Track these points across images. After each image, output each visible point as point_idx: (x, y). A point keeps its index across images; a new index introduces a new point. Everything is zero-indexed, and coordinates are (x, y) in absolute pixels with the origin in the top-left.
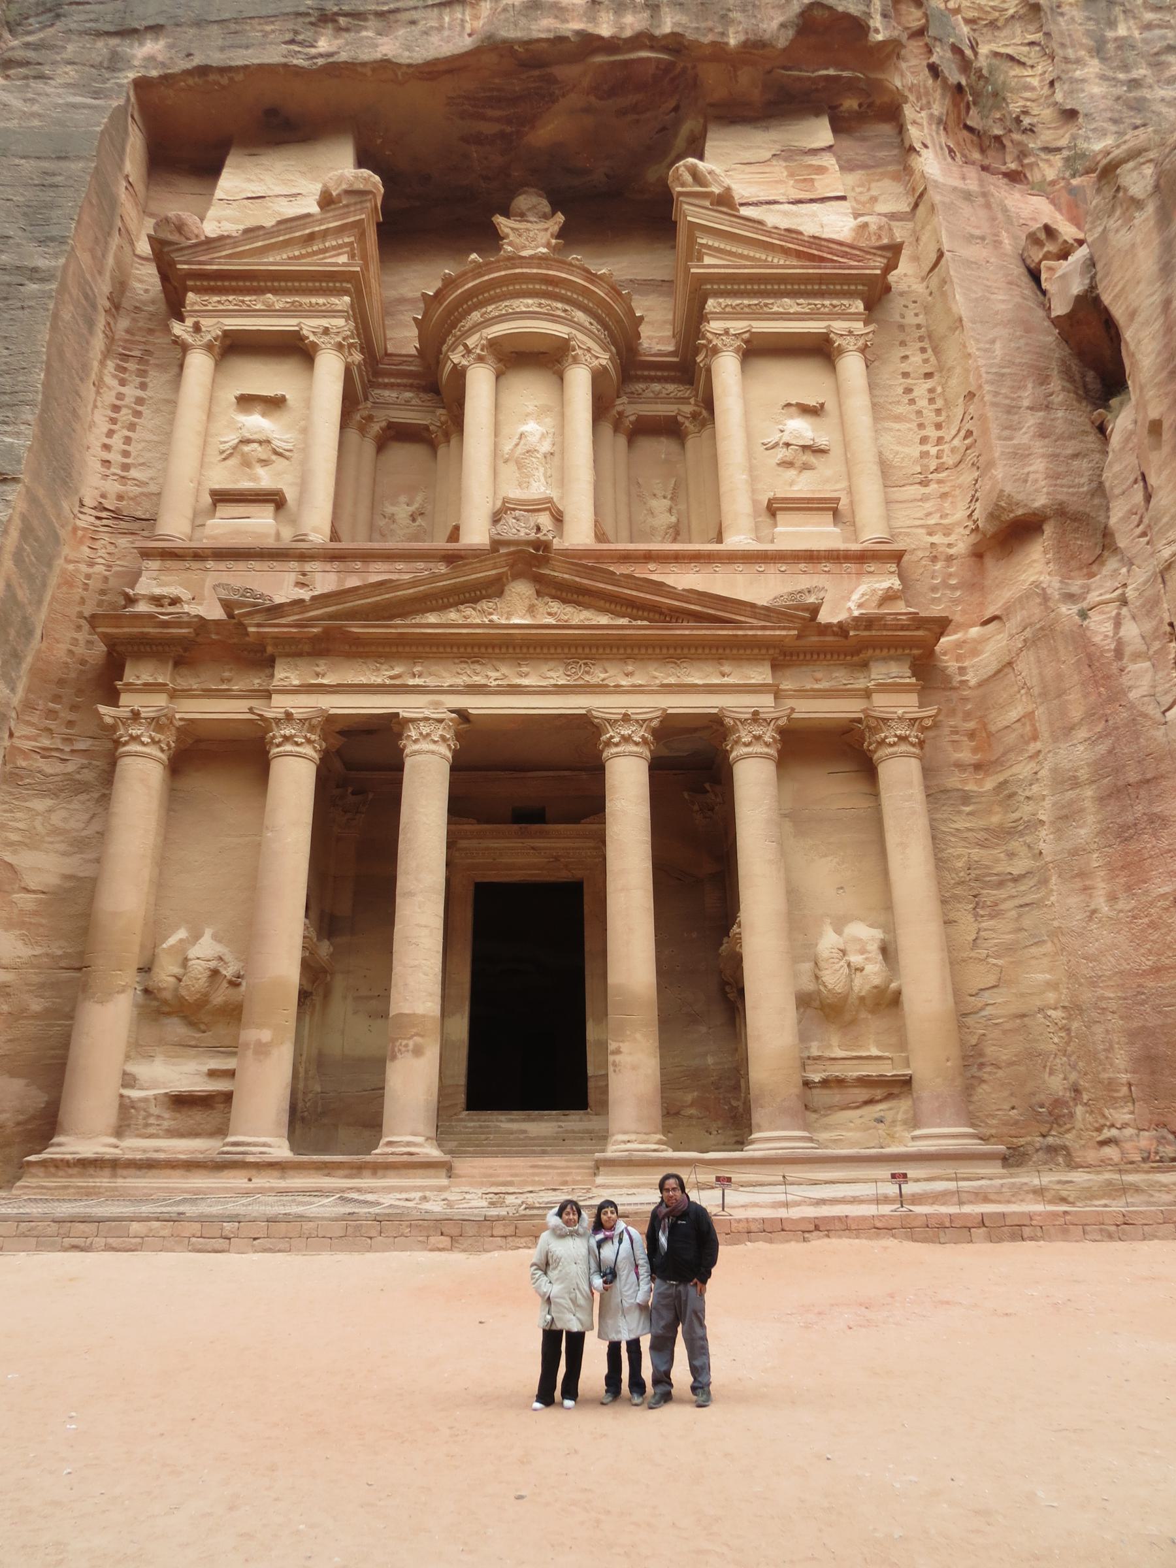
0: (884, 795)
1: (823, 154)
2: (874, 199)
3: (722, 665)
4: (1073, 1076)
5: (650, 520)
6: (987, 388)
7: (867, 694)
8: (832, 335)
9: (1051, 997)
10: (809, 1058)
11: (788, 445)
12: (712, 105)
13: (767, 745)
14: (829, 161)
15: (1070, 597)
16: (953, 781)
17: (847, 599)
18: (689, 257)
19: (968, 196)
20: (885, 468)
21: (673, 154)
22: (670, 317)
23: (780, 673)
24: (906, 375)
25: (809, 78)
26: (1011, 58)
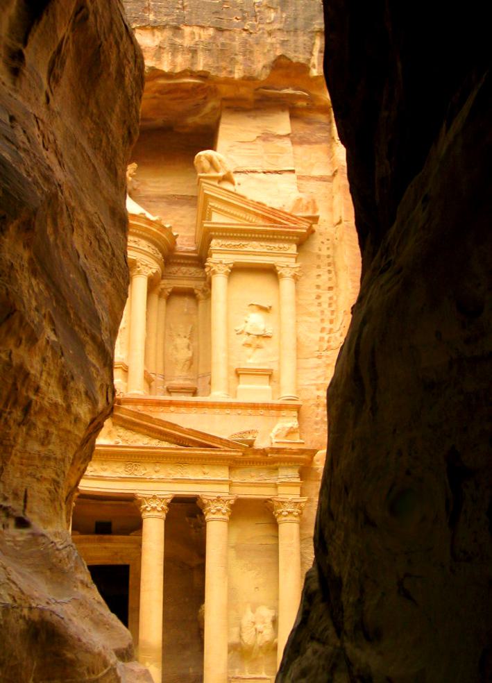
0: (280, 540)
1: (285, 138)
3: (204, 467)
5: (175, 353)
7: (276, 486)
8: (278, 268)
10: (233, 678)
11: (249, 334)
12: (224, 99)
13: (224, 514)
14: (287, 143)
17: (270, 433)
18: (203, 219)
20: (299, 347)
21: (202, 114)
22: (195, 222)
23: (233, 472)
24: (318, 287)
25: (280, 94)
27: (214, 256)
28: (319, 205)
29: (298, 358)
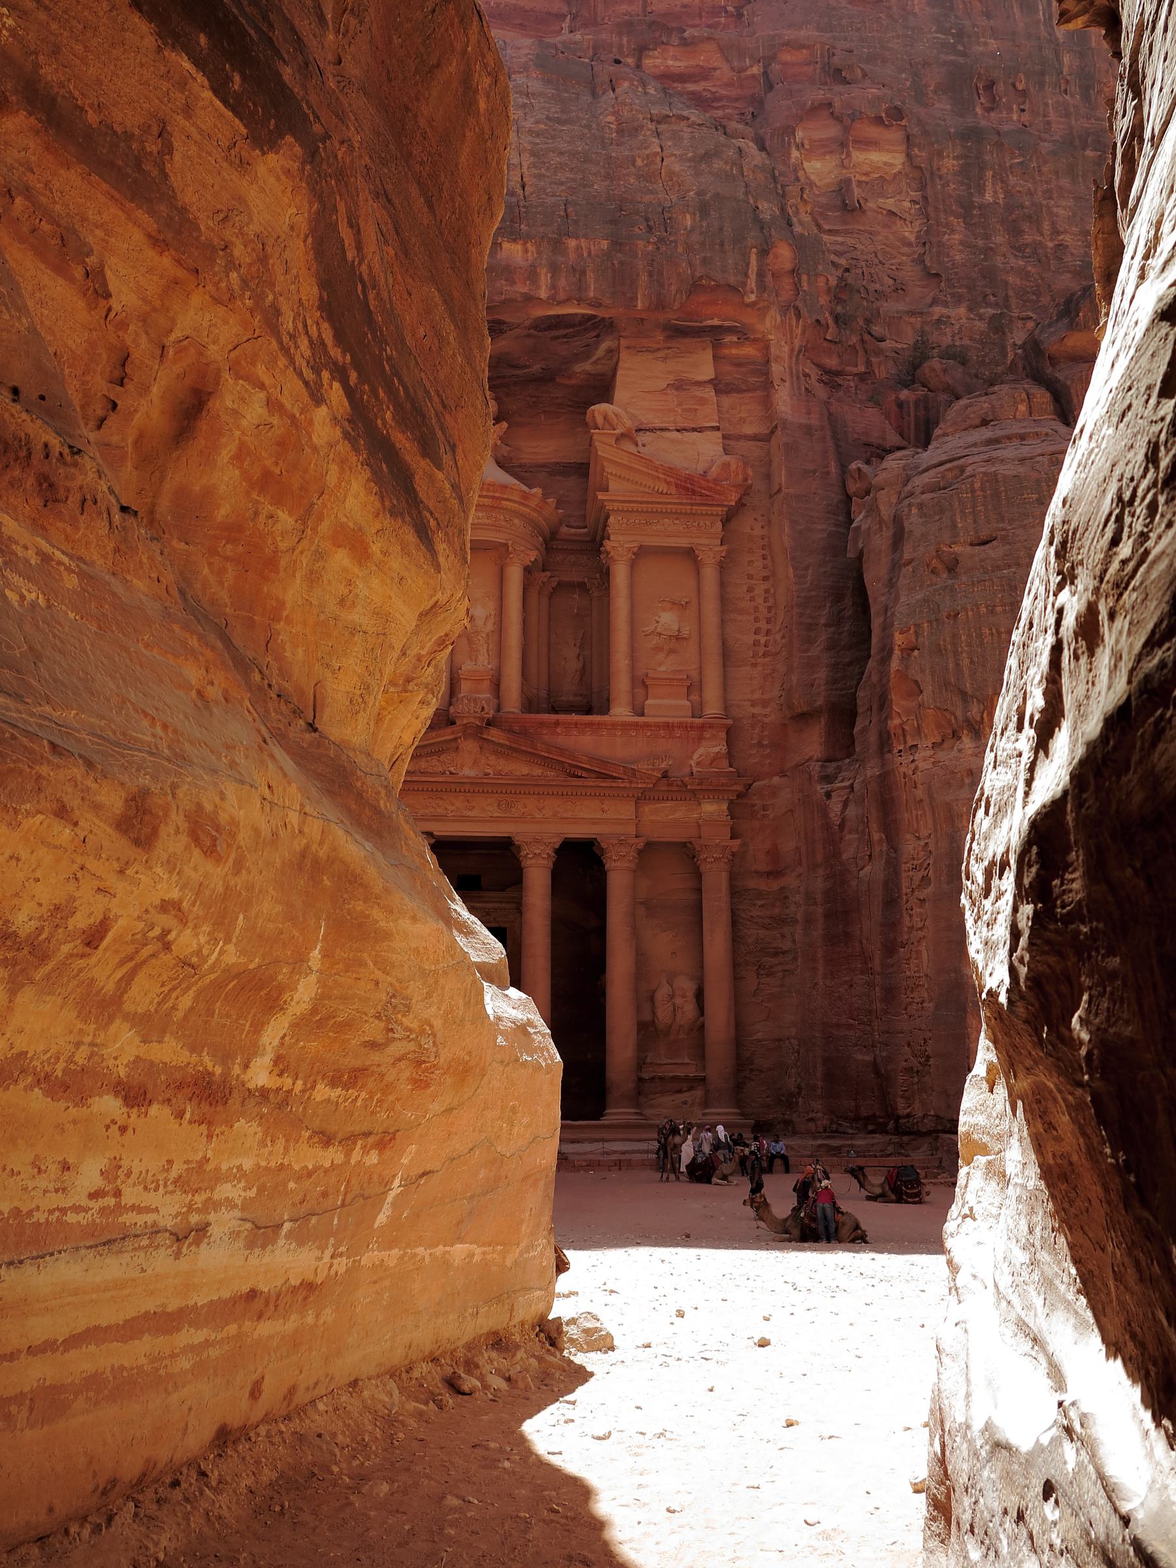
2: (743, 420)
4: (799, 1080)
6: (796, 610)
9: (793, 1031)
11: (660, 634)
13: (630, 861)
14: (709, 393)
15: (828, 779)
16: (752, 883)
19: (808, 430)
20: (726, 655)
21: (595, 358)
24: (750, 577)
26: (891, 213)
27: (612, 538)
28: (750, 472)
29: (724, 665)
